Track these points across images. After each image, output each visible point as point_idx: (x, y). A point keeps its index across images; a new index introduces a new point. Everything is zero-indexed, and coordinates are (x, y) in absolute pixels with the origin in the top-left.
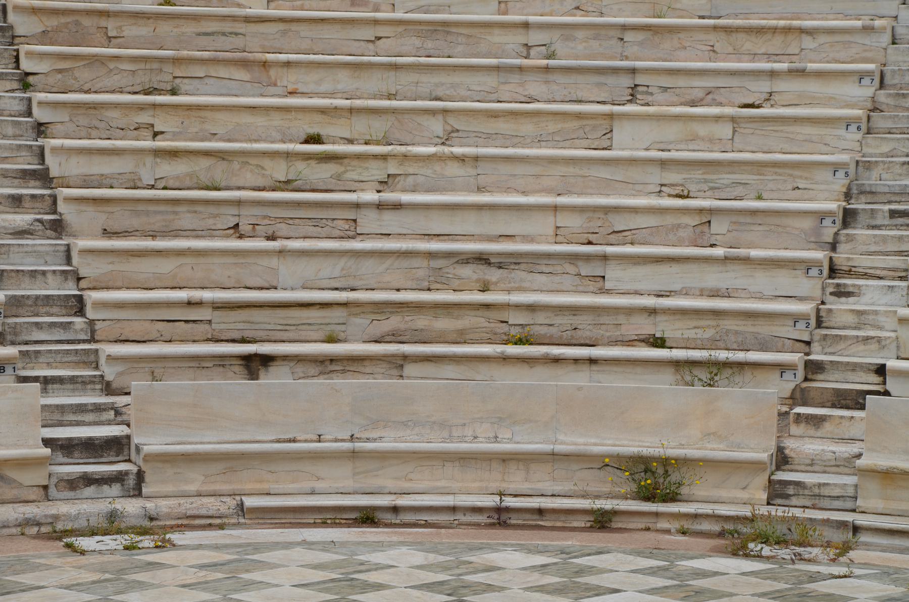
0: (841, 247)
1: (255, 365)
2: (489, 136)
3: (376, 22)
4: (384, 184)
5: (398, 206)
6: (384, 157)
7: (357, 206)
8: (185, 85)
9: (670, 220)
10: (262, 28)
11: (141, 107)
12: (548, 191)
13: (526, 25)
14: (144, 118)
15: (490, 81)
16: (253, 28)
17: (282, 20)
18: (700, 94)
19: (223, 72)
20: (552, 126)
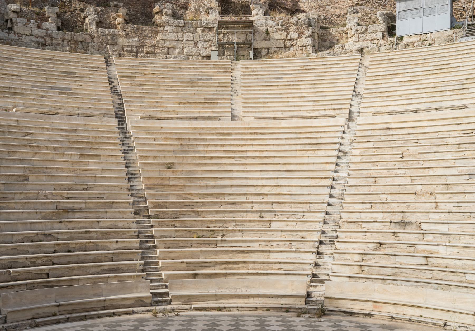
0: (320, 248)
1: (195, 275)
2: (245, 225)
3: (221, 202)
4: (223, 236)
5: (225, 241)
6: (222, 230)
7: (217, 241)
8: (181, 216)
9: (283, 243)
10: (197, 204)
11: (172, 221)
12: (257, 237)
13: (252, 202)
14: (173, 224)
15: (245, 214)
16: (196, 204)
17: (202, 202)
18: (289, 216)
19: (189, 213)
20: (258, 223)
